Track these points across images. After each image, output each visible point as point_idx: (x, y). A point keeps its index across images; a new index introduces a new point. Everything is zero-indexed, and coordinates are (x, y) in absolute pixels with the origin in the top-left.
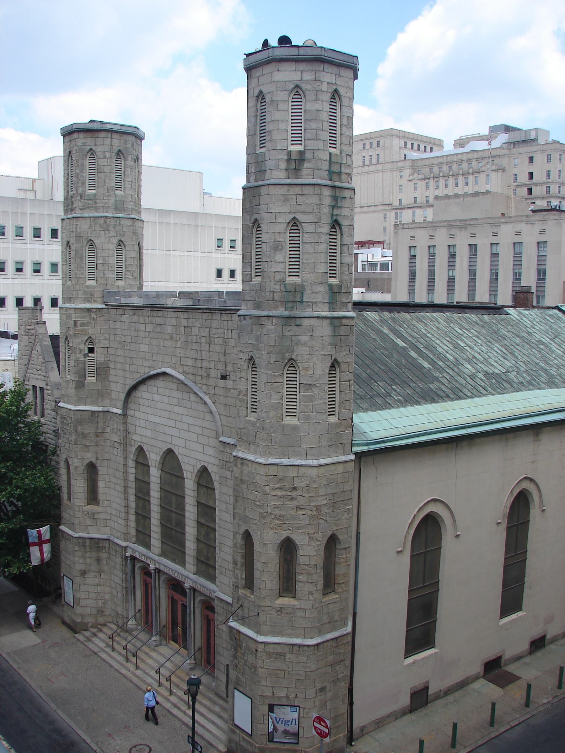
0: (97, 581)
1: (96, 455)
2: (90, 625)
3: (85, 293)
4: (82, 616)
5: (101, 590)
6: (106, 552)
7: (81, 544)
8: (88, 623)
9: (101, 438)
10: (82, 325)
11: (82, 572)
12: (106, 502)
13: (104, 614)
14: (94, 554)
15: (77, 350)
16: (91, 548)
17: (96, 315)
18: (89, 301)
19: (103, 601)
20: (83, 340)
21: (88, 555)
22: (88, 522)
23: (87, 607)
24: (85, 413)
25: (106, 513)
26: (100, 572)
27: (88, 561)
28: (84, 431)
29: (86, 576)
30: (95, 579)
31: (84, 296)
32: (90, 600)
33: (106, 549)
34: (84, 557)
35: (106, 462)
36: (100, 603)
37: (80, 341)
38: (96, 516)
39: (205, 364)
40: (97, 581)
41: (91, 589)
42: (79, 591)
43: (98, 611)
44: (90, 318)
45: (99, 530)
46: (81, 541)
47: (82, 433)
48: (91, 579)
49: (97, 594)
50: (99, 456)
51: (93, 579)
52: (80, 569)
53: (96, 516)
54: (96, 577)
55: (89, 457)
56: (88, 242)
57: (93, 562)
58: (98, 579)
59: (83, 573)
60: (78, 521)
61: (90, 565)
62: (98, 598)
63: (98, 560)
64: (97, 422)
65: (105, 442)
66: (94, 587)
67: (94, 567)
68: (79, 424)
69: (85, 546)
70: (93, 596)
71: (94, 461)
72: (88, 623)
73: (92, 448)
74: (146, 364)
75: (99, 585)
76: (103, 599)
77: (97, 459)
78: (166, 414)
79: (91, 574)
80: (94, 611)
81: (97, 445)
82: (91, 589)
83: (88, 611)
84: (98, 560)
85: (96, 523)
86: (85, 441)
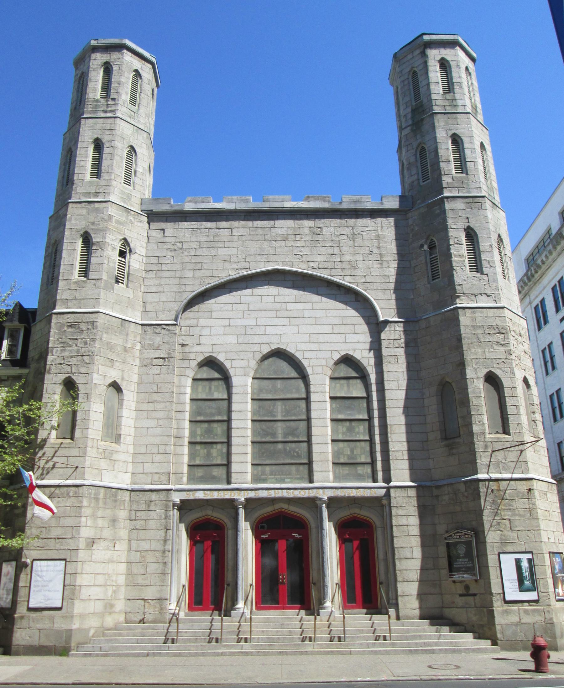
0: (108, 555)
1: (122, 375)
2: (91, 633)
4: (82, 616)
5: (114, 570)
6: (124, 509)
7: (92, 496)
8: (88, 630)
9: (130, 354)
10: (118, 222)
11: (89, 540)
12: (128, 437)
13: (114, 609)
14: (109, 513)
15: (110, 247)
16: (105, 503)
17: (134, 218)
19: (114, 588)
20: (117, 239)
21: (100, 513)
22: (103, 464)
23: (90, 600)
24: (114, 319)
25: (128, 453)
27: (100, 522)
28: (110, 341)
29: (93, 548)
30: (107, 551)
32: (96, 588)
33: (125, 504)
34: (94, 517)
35: (133, 386)
36: (110, 593)
37: (114, 238)
38: (115, 457)
39: (347, 258)
40: (108, 555)
41: (99, 568)
42: (82, 573)
43: (105, 607)
44: (127, 219)
46: (93, 492)
47: (108, 343)
49: (106, 576)
50: (126, 377)
51: (103, 552)
52: (86, 535)
53: (115, 457)
54: (108, 549)
55: (114, 375)
56: (129, 147)
58: (111, 552)
59: (91, 542)
60: (90, 461)
61: (102, 529)
62: (108, 583)
63: (114, 521)
64: (127, 334)
65: (134, 360)
66: (104, 564)
67: (106, 533)
68: (105, 331)
69: (97, 499)
70: (100, 580)
71: (119, 381)
72: (88, 630)
73: (118, 364)
74: (235, 266)
75: (110, 561)
76: (114, 584)
77: (123, 379)
78: (273, 314)
79: (102, 545)
80: (99, 607)
81: (124, 362)
82: (99, 568)
83: (91, 607)
84: (114, 521)
85: (114, 466)
86: (111, 353)
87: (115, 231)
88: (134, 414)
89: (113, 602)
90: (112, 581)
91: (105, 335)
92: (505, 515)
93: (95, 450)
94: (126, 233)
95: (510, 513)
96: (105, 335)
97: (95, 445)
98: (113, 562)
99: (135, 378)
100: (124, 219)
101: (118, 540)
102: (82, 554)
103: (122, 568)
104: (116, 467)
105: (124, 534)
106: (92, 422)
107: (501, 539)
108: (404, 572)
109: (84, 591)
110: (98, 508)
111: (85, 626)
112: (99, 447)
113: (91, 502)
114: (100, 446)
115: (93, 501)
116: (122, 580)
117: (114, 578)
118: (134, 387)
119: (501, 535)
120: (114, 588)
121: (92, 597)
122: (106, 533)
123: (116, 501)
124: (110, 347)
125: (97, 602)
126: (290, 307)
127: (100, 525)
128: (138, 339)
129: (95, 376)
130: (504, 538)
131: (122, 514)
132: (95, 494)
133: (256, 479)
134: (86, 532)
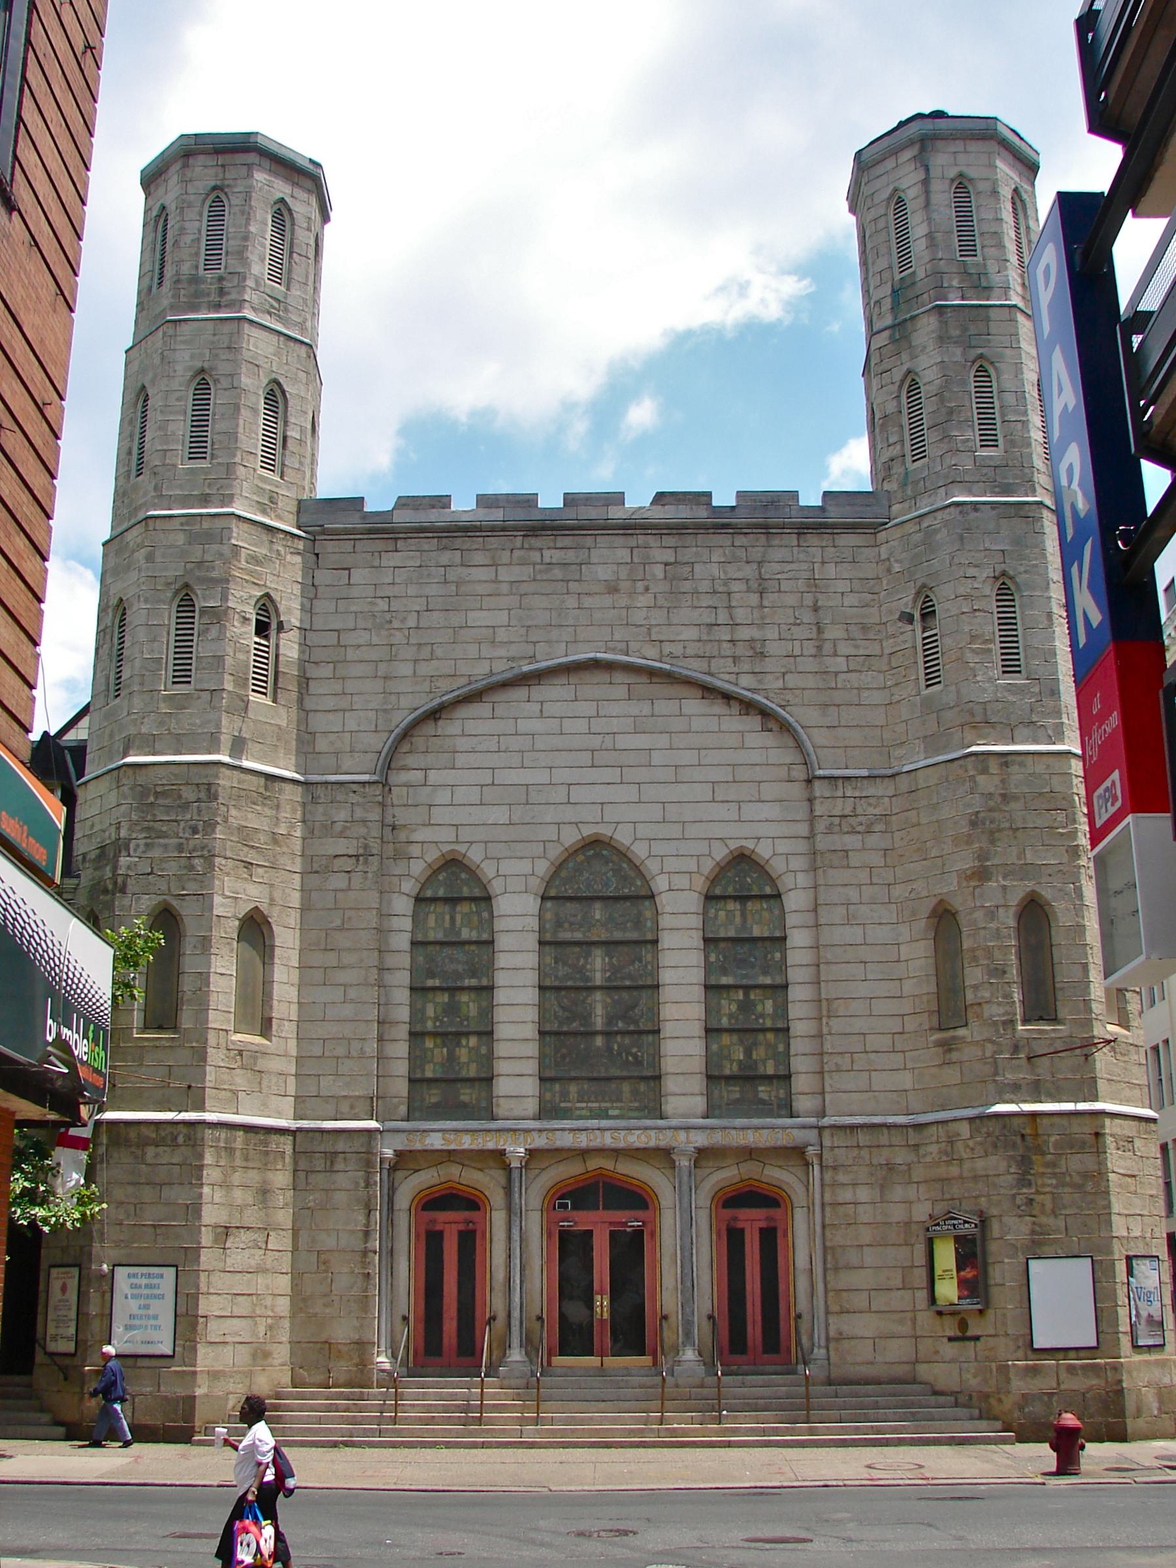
0: (253, 1258)
3: (260, 490)
4: (215, 1375)
5: (267, 1287)
10: (254, 559)
11: (219, 1230)
13: (270, 1360)
14: (254, 1177)
15: (236, 616)
18: (264, 512)
19: (269, 1321)
21: (237, 1178)
22: (241, 1079)
26: (266, 1230)
27: (239, 1195)
30: (253, 1251)
31: (256, 498)
32: (235, 1321)
34: (226, 1185)
36: (262, 1329)
37: (245, 596)
38: (262, 1064)
39: (744, 633)
40: (253, 1258)
41: (240, 1284)
43: (254, 1356)
44: (271, 550)
45: (265, 1105)
48: (240, 1253)
49: (254, 1298)
50: (277, 895)
53: (262, 1064)
55: (253, 894)
57: (250, 1201)
59: (224, 1232)
61: (241, 1208)
62: (258, 1312)
63: (264, 1192)
64: (278, 807)
66: (249, 1275)
67: (251, 1217)
68: (233, 803)
69: (230, 1151)
70: (243, 1306)
71: (264, 908)
73: (260, 871)
74: (502, 652)
75: (261, 1270)
78: (585, 758)
82: (240, 1284)
84: (264, 1192)
87: (247, 581)
88: (295, 976)
89: (268, 1347)
90: (266, 1307)
91: (233, 812)
92: (1043, 1185)
93: (222, 1053)
94: (268, 583)
95: (1054, 1182)
96: (233, 812)
97: (222, 1041)
98: (266, 1271)
99: (295, 899)
100: (263, 551)
101: (275, 1229)
102: (207, 1258)
103: (284, 1283)
104: (265, 1083)
105: (284, 1217)
106: (215, 995)
107: (1033, 1232)
108: (844, 1294)
109: (213, 1325)
110: (234, 1169)
111: (218, 1392)
112: (232, 1047)
113: (219, 1156)
114: (233, 1042)
115: (223, 1154)
116: (283, 1305)
117: (269, 1301)
118: (293, 919)
119: (1034, 1223)
120: (269, 1321)
121: (228, 1339)
122: (251, 1217)
123: (267, 1153)
124: (245, 835)
125: (241, 1346)
126: (623, 741)
127: (239, 1202)
128: (299, 815)
129: (217, 899)
130: (1037, 1228)
131: (281, 1178)
132: (227, 1141)
133: (547, 1111)
134: (211, 1215)
